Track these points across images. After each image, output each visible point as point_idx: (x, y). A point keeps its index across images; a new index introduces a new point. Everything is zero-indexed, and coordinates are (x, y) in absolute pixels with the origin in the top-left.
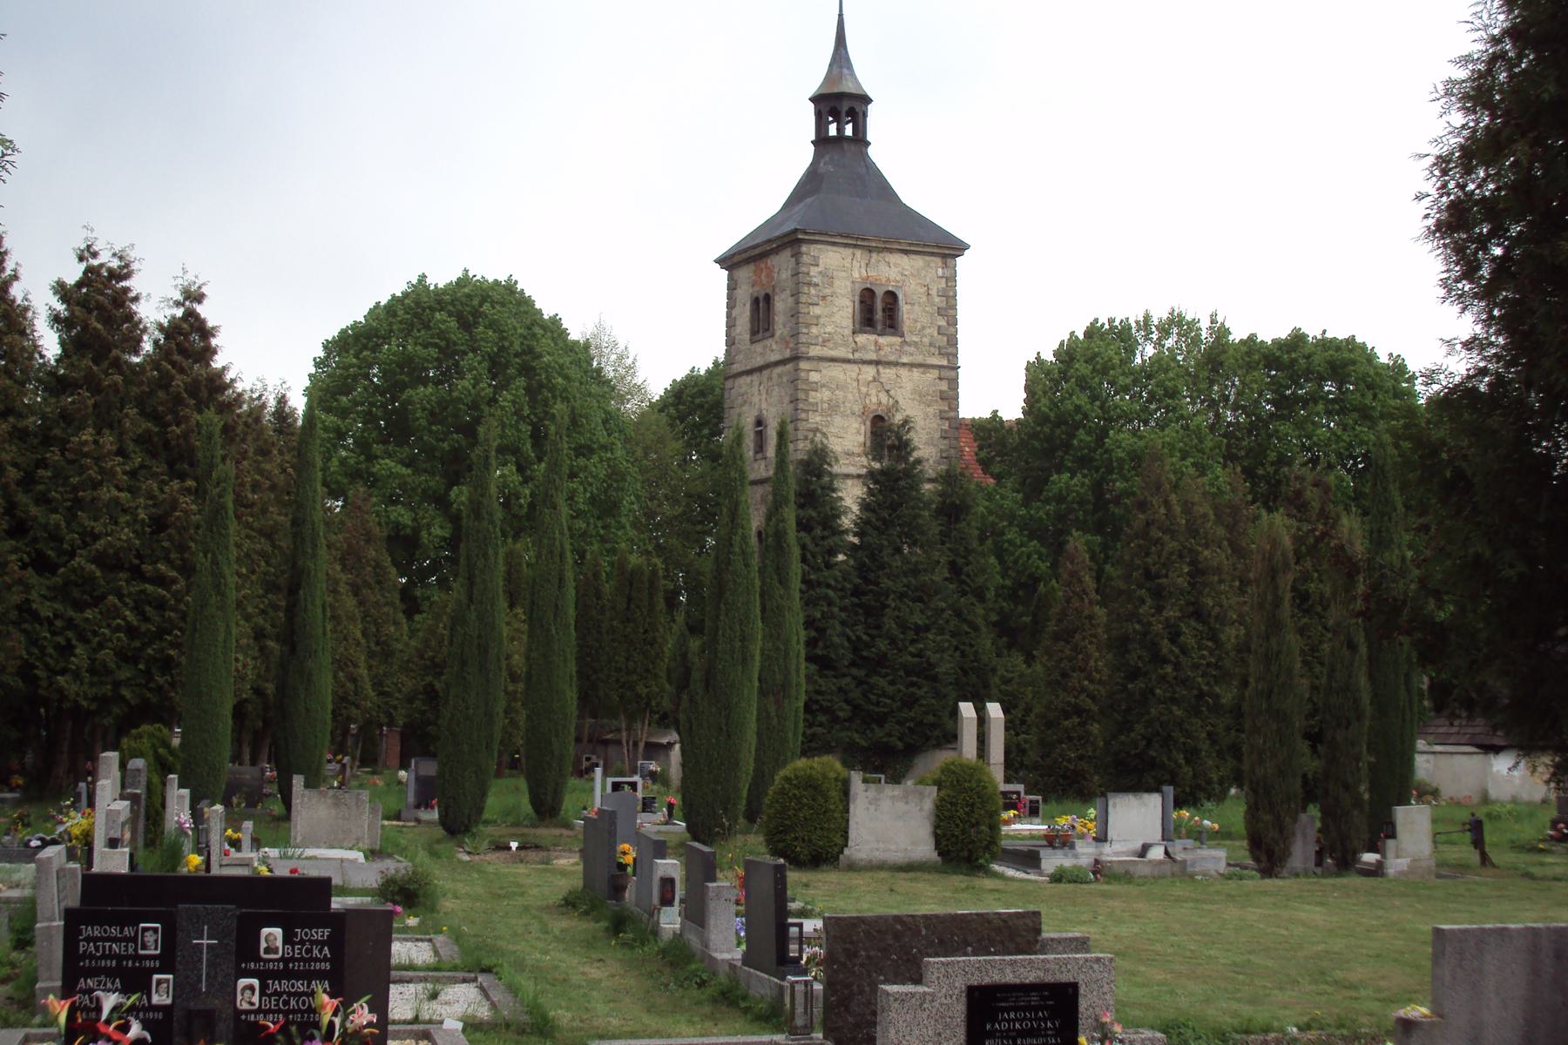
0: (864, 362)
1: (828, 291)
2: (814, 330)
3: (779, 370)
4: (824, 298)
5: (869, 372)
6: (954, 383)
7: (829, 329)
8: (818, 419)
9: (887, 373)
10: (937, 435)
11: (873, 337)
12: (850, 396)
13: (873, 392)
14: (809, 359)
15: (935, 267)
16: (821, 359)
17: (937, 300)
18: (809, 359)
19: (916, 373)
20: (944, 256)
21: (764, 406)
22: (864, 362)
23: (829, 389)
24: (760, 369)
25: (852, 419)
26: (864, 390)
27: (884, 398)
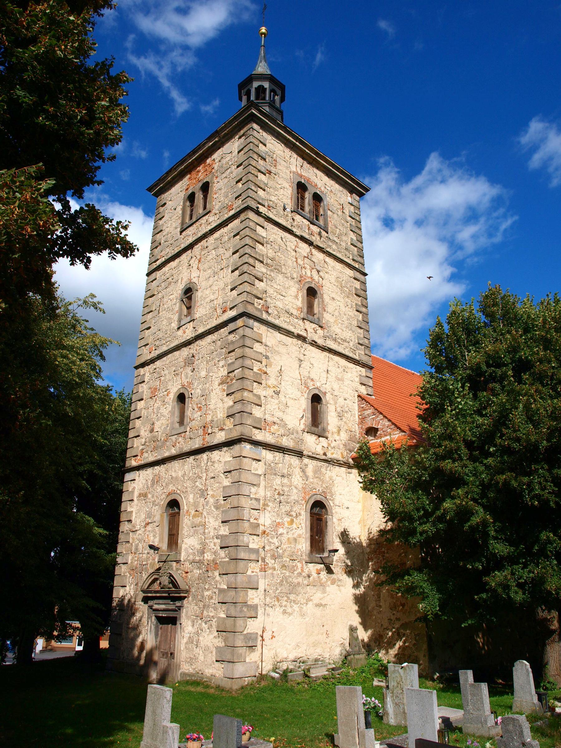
0: (302, 238)
1: (273, 170)
2: (260, 192)
3: (217, 235)
4: (270, 173)
5: (304, 248)
6: (364, 283)
7: (273, 198)
8: (264, 270)
9: (318, 256)
10: (355, 323)
11: (306, 222)
12: (290, 263)
13: (308, 267)
14: (258, 213)
15: (346, 197)
16: (269, 220)
17: (349, 219)
18: (258, 213)
19: (339, 266)
20: (352, 190)
21: (195, 274)
22: (302, 238)
23: (273, 249)
24: (191, 247)
25: (292, 283)
26: (300, 261)
27: (316, 277)
